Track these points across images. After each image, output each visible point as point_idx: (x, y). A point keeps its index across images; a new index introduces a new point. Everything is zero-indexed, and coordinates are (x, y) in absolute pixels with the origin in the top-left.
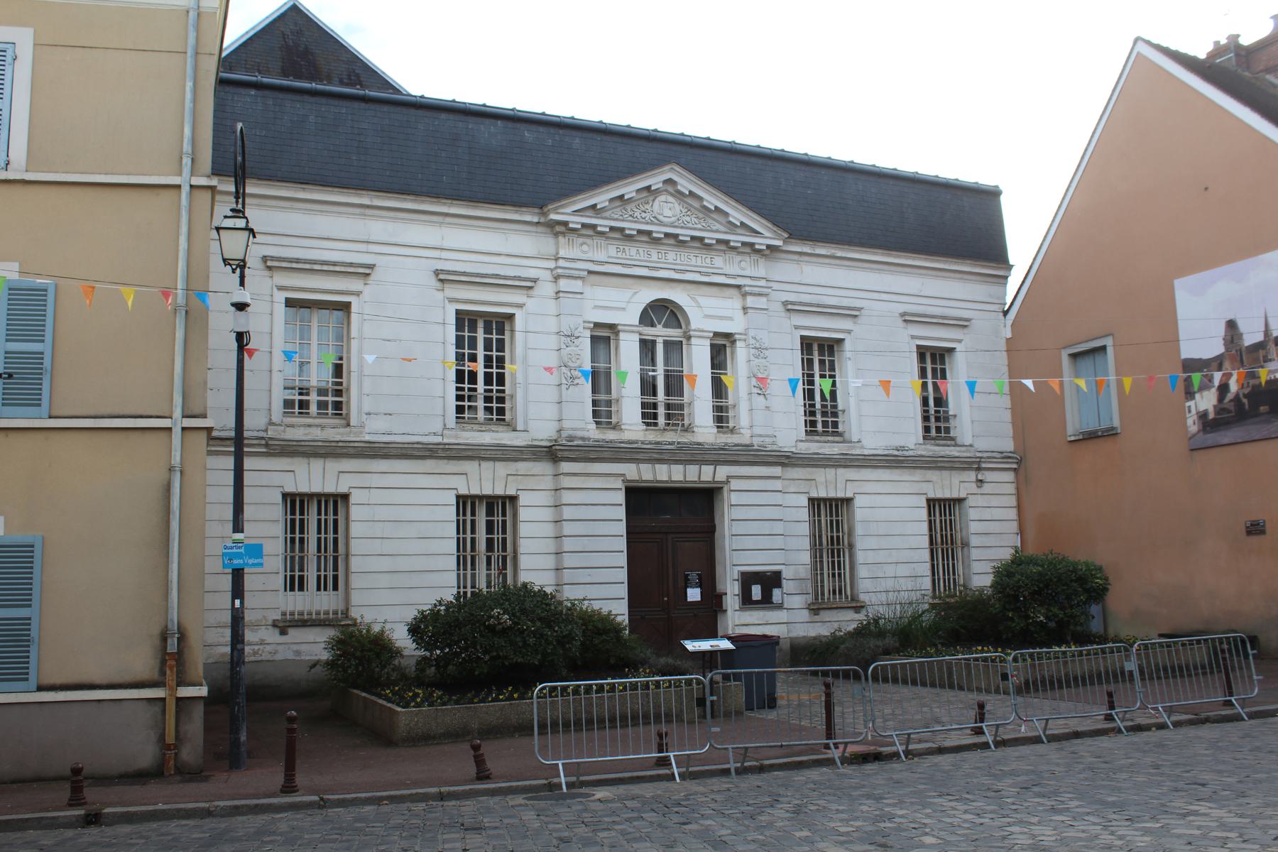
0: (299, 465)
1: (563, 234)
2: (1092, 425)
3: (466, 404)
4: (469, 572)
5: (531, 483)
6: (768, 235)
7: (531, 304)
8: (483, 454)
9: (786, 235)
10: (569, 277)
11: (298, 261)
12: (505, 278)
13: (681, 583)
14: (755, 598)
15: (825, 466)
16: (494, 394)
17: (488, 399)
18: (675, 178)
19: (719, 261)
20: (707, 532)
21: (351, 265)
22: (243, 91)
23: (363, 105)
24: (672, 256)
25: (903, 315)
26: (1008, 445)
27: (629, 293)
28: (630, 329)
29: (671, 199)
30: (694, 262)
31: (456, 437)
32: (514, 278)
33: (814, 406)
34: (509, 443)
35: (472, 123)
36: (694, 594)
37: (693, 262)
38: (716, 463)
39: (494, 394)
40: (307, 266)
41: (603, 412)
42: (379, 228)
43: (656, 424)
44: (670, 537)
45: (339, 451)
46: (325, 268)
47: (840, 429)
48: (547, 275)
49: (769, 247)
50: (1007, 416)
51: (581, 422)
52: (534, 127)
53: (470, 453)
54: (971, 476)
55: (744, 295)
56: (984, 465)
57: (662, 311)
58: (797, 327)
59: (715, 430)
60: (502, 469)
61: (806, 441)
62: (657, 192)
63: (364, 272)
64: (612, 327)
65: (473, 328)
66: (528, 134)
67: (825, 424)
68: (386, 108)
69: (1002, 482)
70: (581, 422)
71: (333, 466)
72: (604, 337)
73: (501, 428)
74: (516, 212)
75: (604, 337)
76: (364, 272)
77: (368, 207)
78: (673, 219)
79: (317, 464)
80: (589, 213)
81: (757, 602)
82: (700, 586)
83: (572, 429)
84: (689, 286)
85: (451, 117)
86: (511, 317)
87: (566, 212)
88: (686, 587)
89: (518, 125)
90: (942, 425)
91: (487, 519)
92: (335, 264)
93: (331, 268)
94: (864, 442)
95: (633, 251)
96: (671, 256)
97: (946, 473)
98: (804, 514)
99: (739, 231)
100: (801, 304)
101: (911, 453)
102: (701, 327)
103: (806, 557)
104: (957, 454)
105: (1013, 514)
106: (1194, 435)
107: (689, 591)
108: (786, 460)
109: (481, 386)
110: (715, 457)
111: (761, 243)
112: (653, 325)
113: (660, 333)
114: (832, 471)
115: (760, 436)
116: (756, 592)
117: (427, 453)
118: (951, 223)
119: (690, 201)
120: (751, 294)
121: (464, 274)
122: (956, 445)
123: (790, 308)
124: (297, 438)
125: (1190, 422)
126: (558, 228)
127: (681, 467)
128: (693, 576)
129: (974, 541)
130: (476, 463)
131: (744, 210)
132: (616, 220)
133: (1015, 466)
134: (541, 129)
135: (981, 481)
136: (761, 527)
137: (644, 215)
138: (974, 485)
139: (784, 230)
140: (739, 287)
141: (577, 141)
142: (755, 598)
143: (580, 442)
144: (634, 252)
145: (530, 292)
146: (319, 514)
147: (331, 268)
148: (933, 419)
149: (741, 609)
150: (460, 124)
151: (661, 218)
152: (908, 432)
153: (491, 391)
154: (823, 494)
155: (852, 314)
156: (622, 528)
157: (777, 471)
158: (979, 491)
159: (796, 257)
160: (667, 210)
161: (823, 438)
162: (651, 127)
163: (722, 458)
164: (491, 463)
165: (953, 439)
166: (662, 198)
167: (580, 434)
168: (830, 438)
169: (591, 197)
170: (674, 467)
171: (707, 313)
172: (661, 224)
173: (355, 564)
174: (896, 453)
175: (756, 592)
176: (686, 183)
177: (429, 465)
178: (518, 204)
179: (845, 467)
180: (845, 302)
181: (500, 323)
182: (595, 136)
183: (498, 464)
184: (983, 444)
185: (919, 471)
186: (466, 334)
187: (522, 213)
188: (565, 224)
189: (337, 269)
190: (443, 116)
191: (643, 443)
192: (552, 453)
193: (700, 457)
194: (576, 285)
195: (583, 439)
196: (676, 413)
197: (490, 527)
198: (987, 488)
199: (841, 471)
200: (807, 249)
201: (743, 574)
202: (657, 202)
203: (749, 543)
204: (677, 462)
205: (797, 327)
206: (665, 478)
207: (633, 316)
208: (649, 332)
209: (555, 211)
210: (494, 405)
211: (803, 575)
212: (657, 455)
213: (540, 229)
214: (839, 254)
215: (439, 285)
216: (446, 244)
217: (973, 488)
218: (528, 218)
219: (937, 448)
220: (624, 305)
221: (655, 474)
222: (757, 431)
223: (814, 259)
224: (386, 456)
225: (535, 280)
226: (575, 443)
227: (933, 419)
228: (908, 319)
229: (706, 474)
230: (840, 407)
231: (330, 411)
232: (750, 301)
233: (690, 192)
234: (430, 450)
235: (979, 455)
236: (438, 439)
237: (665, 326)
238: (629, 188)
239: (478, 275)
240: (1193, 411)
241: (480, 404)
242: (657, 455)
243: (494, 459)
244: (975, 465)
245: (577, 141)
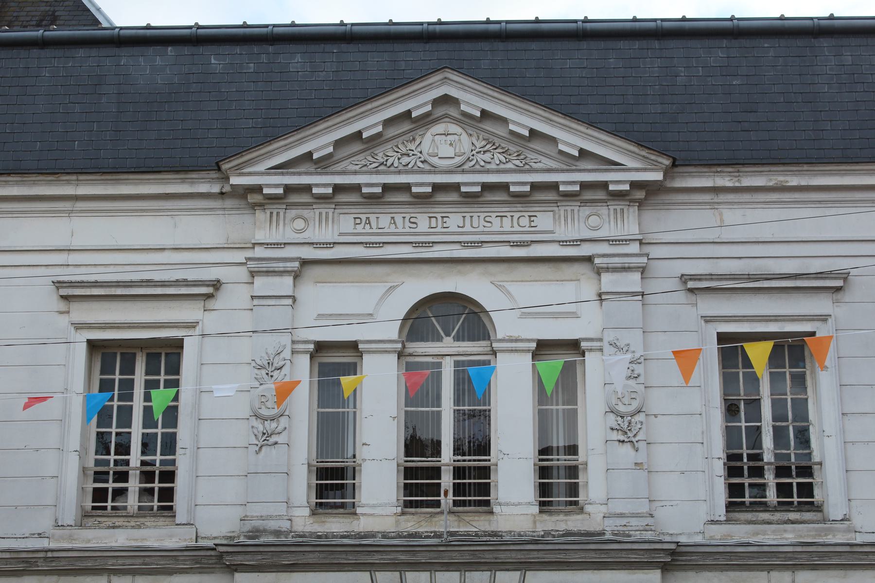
1: (261, 205)
3: (111, 485)
6: (633, 166)
7: (211, 321)
8: (110, 564)
9: (667, 162)
10: (268, 273)
12: (163, 284)
15: (769, 568)
16: (157, 469)
17: (147, 476)
18: (454, 92)
19: (544, 220)
27: (381, 288)
28: (380, 347)
29: (454, 128)
30: (499, 224)
31: (71, 538)
32: (177, 283)
33: (758, 457)
34: (156, 544)
37: (496, 227)
39: (157, 469)
41: (333, 483)
43: (437, 504)
47: (818, 496)
48: (242, 273)
49: (635, 185)
52: (225, 49)
53: (89, 564)
55: (599, 271)
58: (708, 320)
59: (536, 509)
61: (728, 521)
62: (426, 121)
64: (353, 346)
65: (129, 368)
66: (216, 60)
72: (335, 361)
73: (119, 522)
74: (183, 181)
75: (335, 361)
78: (458, 160)
83: (262, 518)
84: (493, 268)
85: (94, 52)
86: (178, 344)
87: (260, 172)
89: (201, 49)
94: (858, 521)
96: (454, 221)
100: (711, 277)
102: (515, 334)
109: (135, 457)
110: (520, 557)
112: (439, 339)
113: (447, 350)
115: (621, 515)
117: (21, 566)
119: (488, 126)
120: (607, 270)
121: (96, 284)
123: (695, 287)
126: (253, 198)
131: (582, 128)
132: (355, 173)
134: (238, 49)
139: (662, 153)
140: (589, 259)
141: (298, 58)
143: (271, 539)
145: (211, 304)
151: (435, 161)
153: (152, 463)
155: (834, 285)
159: (707, 197)
160: (445, 148)
161: (778, 516)
162: (480, 16)
163: (534, 557)
166: (439, 128)
167: (273, 525)
168: (793, 516)
169: (301, 142)
172: (434, 170)
176: (473, 99)
179: (814, 567)
180: (816, 266)
181: (165, 356)
182: (328, 47)
186: (117, 377)
187: (192, 182)
188: (258, 189)
190: (81, 52)
191: (385, 536)
194: (285, 285)
195: (277, 533)
196: (475, 487)
202: (429, 136)
205: (708, 319)
207: (390, 330)
208: (423, 348)
209: (238, 170)
213: (229, 203)
214: (747, 182)
216: (77, 243)
218: (203, 188)
220: (372, 308)
222: (618, 507)
223: (746, 197)
225: (217, 285)
226: (263, 540)
230: (816, 457)
232: (608, 281)
233: (484, 112)
234: (25, 561)
236: (44, 544)
237: (457, 338)
238: (369, 121)
239: (118, 284)
241: (134, 484)
243: (133, 572)
245: (298, 58)
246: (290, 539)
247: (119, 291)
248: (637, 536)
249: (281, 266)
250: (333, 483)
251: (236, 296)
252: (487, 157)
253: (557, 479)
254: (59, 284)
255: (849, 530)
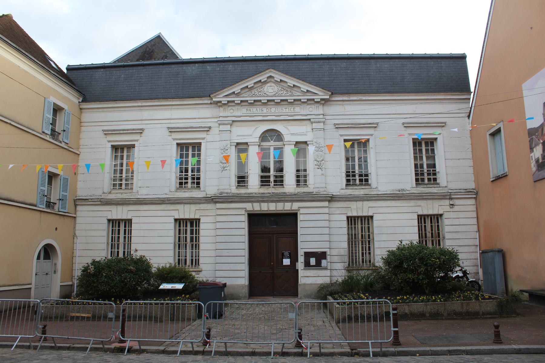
0: (113, 208)
2: (500, 174)
3: (184, 181)
4: (126, 250)
5: (206, 213)
6: (321, 94)
7: (209, 137)
8: (184, 201)
9: (330, 93)
10: (224, 124)
11: (114, 130)
12: (196, 128)
13: (280, 257)
14: (311, 264)
15: (357, 201)
16: (196, 177)
17: (193, 179)
18: (272, 75)
20: (295, 233)
21: (134, 130)
22: (99, 70)
23: (142, 67)
24: (274, 110)
25: (403, 124)
26: (471, 185)
27: (254, 128)
29: (273, 84)
30: (285, 111)
31: (174, 195)
32: (199, 127)
33: (354, 172)
34: (196, 196)
35: (185, 67)
36: (286, 262)
37: (284, 111)
38: (292, 201)
39: (196, 177)
40: (118, 132)
41: (242, 180)
42: (147, 114)
43: (270, 185)
44: (275, 236)
45: (127, 202)
46: (125, 132)
47: (370, 182)
48: (217, 125)
49: (322, 99)
50: (471, 170)
51: (230, 186)
52: (212, 64)
53: (179, 201)
54: (447, 202)
56: (453, 197)
57: (266, 136)
60: (193, 207)
61: (346, 189)
62: (265, 83)
63: (141, 132)
64: (247, 143)
65: (187, 150)
66: (209, 67)
67: (429, 180)
68: (151, 67)
69: (467, 206)
70: (230, 186)
71: (126, 208)
73: (186, 190)
75: (242, 147)
76: (141, 132)
77: (142, 106)
78: (274, 93)
79: (120, 208)
80: (234, 96)
81: (313, 266)
82: (290, 258)
83: (223, 189)
84: (284, 122)
85: (177, 66)
86: (200, 143)
87: (220, 97)
88: (283, 259)
90: (432, 177)
91: (120, 227)
92: (128, 130)
93: (127, 132)
94: (380, 188)
95: (254, 110)
96: (273, 110)
97: (430, 202)
98: (345, 224)
99: (308, 94)
100: (342, 124)
101: (407, 192)
102: (290, 140)
103: (345, 245)
104: (436, 192)
105: (474, 221)
106: (534, 173)
107: (284, 260)
108: (332, 199)
109: (190, 174)
111: (317, 98)
112: (270, 141)
113: (271, 144)
114: (361, 203)
115: (318, 188)
116: (313, 261)
118: (441, 75)
119: (282, 84)
120: (314, 122)
121: (178, 128)
122: (440, 187)
123: (338, 127)
124: (185, 196)
125: (532, 165)
126: (219, 104)
127: (274, 204)
128: (286, 253)
129: (447, 236)
130: (182, 206)
131: (307, 84)
133: (475, 196)
134: (215, 64)
135: (452, 205)
136: (320, 231)
137: (260, 93)
138: (448, 207)
139: (329, 91)
140: (310, 120)
141: (231, 66)
142: (311, 264)
144: (254, 110)
145: (208, 133)
146: (113, 227)
147: (127, 132)
148: (426, 175)
149: (304, 269)
150: (180, 68)
151: (267, 93)
152: (407, 181)
153: (194, 175)
154: (355, 214)
155: (374, 126)
156: (246, 232)
157: (326, 204)
158: (451, 210)
160: (270, 90)
161: (359, 187)
164: (189, 205)
165: (438, 184)
166: (269, 84)
167: (226, 191)
168: (363, 187)
169: (232, 89)
170: (262, 204)
171: (291, 133)
172: (268, 96)
173: (376, 244)
174: (398, 192)
175: (313, 261)
176: (278, 76)
177: (163, 207)
178: (200, 97)
179: (368, 200)
182: (239, 63)
183: (192, 206)
184: (454, 186)
185: (413, 201)
186: (184, 152)
187: (203, 100)
188: (220, 102)
189: (129, 132)
190: (173, 66)
191: (255, 194)
192: (212, 200)
193: (283, 199)
194: (228, 127)
195: (227, 193)
196: (279, 181)
197: (192, 231)
198: (456, 208)
199: (365, 203)
200: (345, 98)
201: (305, 253)
202: (266, 86)
203: (309, 238)
204: (272, 202)
205: (341, 136)
206: (266, 209)
208: (265, 144)
210: (196, 181)
211: (343, 254)
212: (261, 199)
213: (213, 106)
214: (352, 98)
215: (170, 134)
216: (173, 117)
217: (448, 208)
218: (206, 102)
219: (423, 189)
220: (251, 134)
221: (276, 208)
223: (351, 103)
224: (141, 204)
225: (210, 128)
227: (426, 175)
228: (407, 126)
229: (295, 206)
230: (369, 172)
231: (117, 187)
232: (315, 125)
234: (162, 201)
235: (450, 191)
236: (167, 196)
237: (274, 141)
238: (250, 83)
239: (184, 128)
240: (534, 159)
241: (190, 181)
242: (261, 199)
244: (449, 196)
245: (231, 66)
246: (231, 195)
247: (184, 130)
248: (322, 193)
249: (226, 122)
250: (242, 180)
251: (215, 131)
252: (282, 92)
253: (301, 178)
254: (169, 128)
255: (377, 191)
